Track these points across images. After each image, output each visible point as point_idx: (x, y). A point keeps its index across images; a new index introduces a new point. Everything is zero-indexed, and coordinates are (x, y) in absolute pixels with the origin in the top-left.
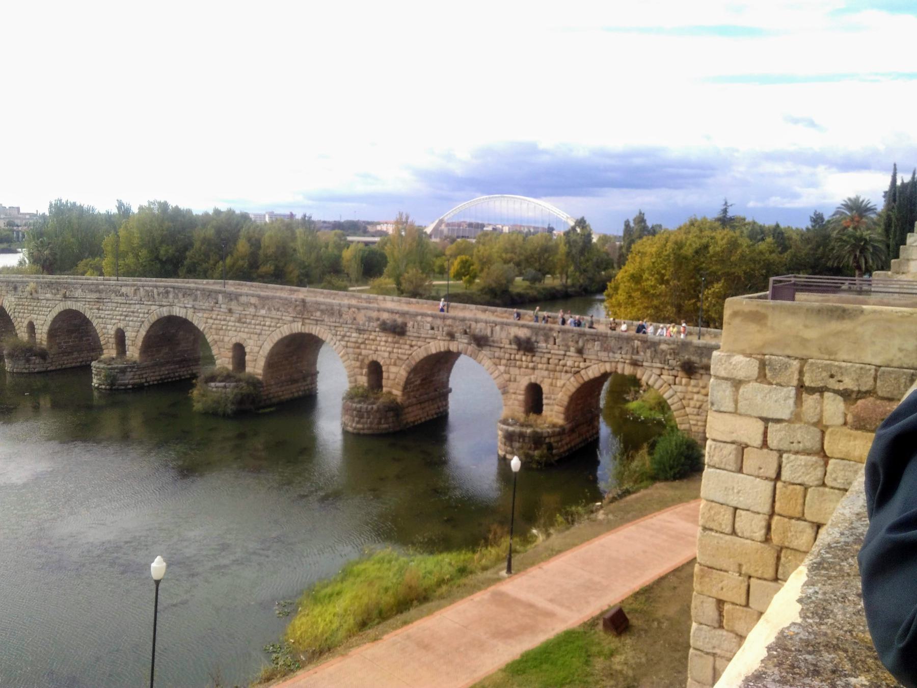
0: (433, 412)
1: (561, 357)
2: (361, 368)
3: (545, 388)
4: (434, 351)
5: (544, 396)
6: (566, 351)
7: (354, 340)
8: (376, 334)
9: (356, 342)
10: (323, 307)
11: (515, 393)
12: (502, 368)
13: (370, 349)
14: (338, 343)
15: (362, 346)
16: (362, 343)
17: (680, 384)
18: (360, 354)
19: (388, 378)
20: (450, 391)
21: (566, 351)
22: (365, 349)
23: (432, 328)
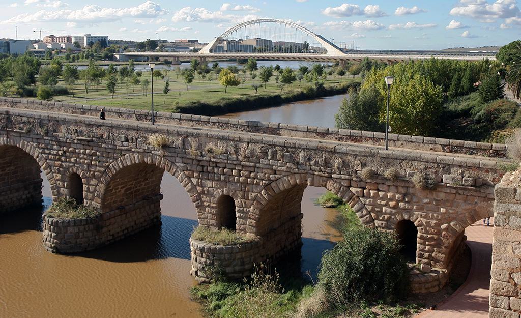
0: (142, 220)
1: (252, 169)
2: (63, 181)
3: (237, 202)
4: (129, 164)
5: (237, 209)
6: (256, 163)
7: (55, 152)
8: (75, 146)
9: (57, 154)
10: (25, 119)
11: (209, 206)
12: (194, 180)
13: (70, 162)
14: (40, 155)
15: (63, 159)
16: (62, 156)
17: (369, 196)
18: (61, 166)
19: (88, 190)
20: (162, 197)
21: (256, 163)
22: (66, 161)
23: (127, 140)
